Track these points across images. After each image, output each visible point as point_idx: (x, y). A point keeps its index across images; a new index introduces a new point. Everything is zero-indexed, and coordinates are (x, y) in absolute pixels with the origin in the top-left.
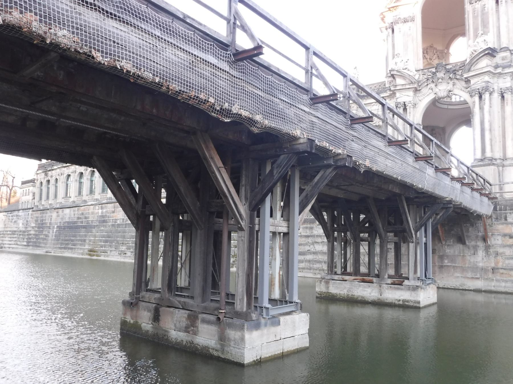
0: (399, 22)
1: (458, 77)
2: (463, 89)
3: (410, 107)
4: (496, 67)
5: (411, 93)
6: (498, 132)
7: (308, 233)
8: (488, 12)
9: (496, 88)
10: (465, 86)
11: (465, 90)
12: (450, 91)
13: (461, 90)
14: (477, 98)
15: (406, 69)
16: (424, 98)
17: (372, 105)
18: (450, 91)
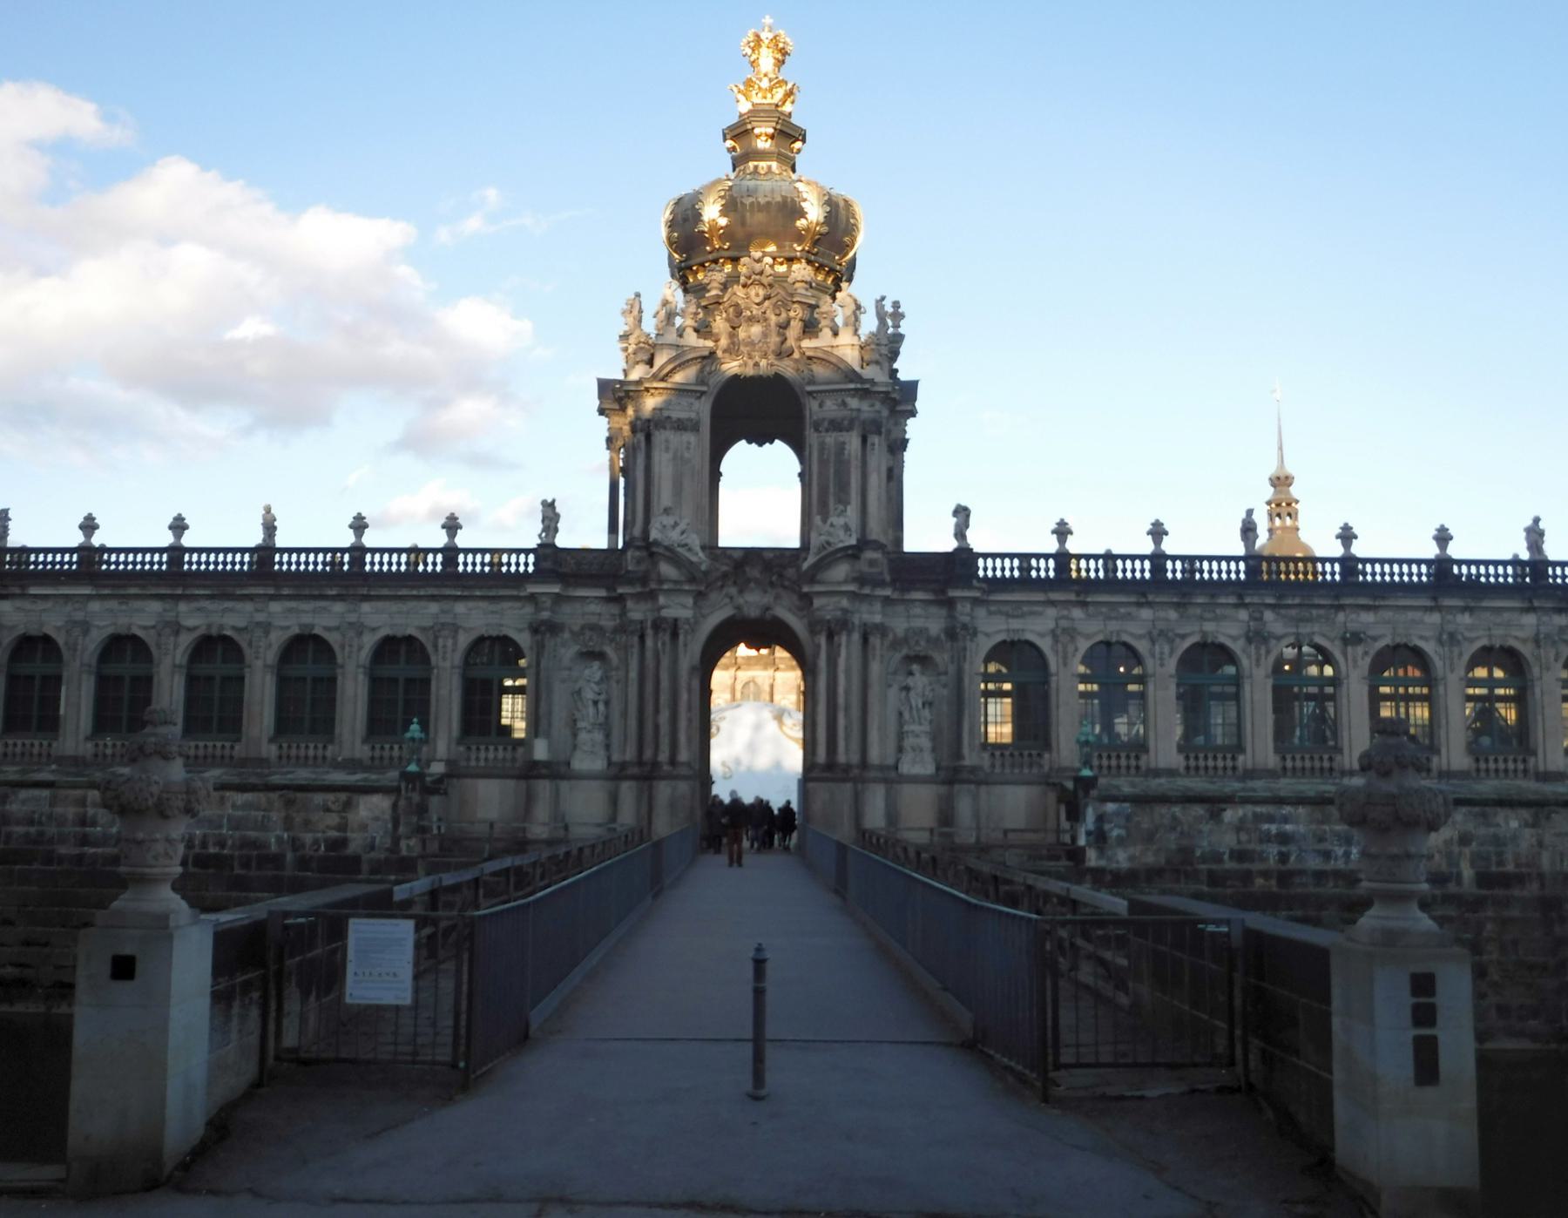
1: (787, 583)
3: (686, 632)
4: (861, 580)
5: (690, 601)
6: (855, 712)
8: (849, 462)
9: (857, 622)
13: (790, 610)
14: (823, 640)
15: (686, 545)
16: (712, 612)
17: (588, 601)
18: (768, 609)
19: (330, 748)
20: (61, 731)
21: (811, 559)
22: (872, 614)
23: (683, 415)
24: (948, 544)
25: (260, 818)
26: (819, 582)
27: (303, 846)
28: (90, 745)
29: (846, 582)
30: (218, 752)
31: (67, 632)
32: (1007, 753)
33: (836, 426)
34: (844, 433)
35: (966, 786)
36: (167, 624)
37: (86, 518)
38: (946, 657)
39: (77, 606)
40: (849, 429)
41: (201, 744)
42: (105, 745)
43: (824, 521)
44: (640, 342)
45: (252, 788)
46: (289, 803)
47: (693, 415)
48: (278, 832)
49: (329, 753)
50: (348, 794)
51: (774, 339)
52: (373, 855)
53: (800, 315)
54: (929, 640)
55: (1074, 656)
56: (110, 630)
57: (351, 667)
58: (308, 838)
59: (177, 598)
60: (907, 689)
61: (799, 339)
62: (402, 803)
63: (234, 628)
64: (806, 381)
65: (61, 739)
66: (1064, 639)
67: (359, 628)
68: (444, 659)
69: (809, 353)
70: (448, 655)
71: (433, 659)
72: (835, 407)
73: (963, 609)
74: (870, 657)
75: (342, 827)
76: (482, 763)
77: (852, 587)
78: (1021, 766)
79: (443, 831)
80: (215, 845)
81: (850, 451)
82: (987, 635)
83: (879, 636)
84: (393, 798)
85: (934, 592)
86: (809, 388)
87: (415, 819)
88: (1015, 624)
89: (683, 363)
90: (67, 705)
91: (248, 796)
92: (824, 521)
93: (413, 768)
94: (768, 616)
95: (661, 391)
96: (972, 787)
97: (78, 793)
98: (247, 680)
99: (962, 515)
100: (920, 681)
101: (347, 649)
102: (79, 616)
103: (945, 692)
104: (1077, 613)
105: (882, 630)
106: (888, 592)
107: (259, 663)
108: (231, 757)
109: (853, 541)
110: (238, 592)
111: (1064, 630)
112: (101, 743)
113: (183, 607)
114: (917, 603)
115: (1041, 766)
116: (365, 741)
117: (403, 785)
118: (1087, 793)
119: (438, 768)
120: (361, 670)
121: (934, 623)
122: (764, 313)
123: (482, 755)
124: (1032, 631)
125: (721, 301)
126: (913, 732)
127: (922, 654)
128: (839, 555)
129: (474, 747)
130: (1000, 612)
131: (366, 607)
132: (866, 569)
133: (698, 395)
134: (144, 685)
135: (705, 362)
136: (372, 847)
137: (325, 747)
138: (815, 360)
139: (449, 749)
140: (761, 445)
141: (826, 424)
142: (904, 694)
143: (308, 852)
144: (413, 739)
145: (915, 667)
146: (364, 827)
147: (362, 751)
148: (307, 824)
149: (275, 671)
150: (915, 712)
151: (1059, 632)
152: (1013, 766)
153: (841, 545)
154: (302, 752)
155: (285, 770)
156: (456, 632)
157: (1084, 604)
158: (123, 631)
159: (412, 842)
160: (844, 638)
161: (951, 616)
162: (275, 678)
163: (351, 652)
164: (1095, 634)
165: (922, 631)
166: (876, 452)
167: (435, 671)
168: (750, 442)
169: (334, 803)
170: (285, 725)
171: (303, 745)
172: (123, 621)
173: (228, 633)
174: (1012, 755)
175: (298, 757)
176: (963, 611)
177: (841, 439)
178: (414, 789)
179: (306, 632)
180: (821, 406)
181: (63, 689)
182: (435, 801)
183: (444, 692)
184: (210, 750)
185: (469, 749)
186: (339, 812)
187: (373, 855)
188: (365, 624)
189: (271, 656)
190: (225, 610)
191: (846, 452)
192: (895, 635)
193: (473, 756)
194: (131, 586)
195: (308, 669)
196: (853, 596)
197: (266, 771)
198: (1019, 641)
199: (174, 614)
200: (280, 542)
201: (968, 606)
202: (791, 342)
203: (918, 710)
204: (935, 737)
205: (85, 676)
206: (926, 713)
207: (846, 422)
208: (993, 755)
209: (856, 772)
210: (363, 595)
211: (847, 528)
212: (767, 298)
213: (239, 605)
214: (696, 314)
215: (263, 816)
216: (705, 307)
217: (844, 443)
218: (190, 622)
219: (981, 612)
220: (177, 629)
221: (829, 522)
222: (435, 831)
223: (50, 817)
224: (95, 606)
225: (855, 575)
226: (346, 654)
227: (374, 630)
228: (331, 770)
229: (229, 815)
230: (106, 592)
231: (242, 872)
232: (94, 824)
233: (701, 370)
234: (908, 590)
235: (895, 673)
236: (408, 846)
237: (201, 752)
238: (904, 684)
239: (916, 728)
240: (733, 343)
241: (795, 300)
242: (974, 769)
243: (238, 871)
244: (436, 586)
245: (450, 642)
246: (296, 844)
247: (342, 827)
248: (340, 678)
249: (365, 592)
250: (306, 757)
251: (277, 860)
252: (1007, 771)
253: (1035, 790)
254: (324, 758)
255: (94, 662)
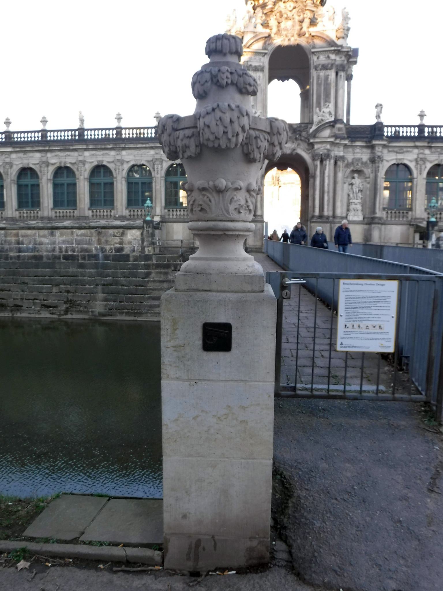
0: (251, 69)
1: (303, 138)
2: (305, 150)
4: (336, 137)
6: (331, 194)
7: (162, 278)
9: (333, 155)
10: (307, 147)
11: (307, 151)
12: (294, 150)
13: (304, 150)
14: (318, 163)
19: (113, 211)
20: (6, 207)
21: (314, 128)
22: (339, 152)
23: (257, 64)
24: (371, 121)
25: (88, 240)
26: (318, 138)
27: (106, 251)
28: (17, 213)
29: (329, 137)
30: (68, 214)
31: (4, 167)
32: (393, 212)
33: (325, 67)
34: (328, 71)
35: (377, 225)
36: (43, 162)
37: (7, 119)
38: (369, 170)
39: (7, 156)
40: (330, 69)
41: (61, 211)
42: (23, 213)
43: (320, 111)
44: (237, 31)
45: (85, 228)
46: (99, 233)
47: (261, 64)
48: (96, 245)
49: (112, 214)
50: (123, 230)
51: (298, 28)
52: (134, 254)
53: (309, 17)
54: (362, 163)
55: (424, 170)
56: (21, 166)
57: (119, 178)
58: (108, 247)
59: (46, 151)
60: (352, 184)
61: (308, 28)
62: (145, 233)
63: (71, 163)
64: (312, 47)
65: (6, 210)
66: (421, 163)
67: (122, 162)
68: (157, 173)
69: (313, 34)
70: (159, 172)
71: (153, 174)
72: (324, 59)
73: (378, 149)
74: (338, 171)
75: (121, 243)
76: (175, 217)
77: (332, 140)
78: (399, 217)
79: (160, 244)
80: (71, 251)
81: (331, 79)
82: (387, 161)
83: (342, 161)
84: (141, 231)
85: (366, 142)
86: (313, 50)
87: (150, 239)
88: (400, 156)
89: (259, 39)
90: (7, 196)
91: (83, 231)
92: (320, 111)
93: (148, 218)
94: (294, 153)
95: (247, 53)
96: (380, 226)
97: (15, 231)
98: (77, 185)
99: (379, 108)
100: (357, 181)
101: (117, 170)
102: (8, 160)
103: (368, 186)
104: (427, 151)
105: (343, 158)
106: (346, 142)
107: (82, 177)
108: (73, 216)
109: (332, 119)
110: (71, 148)
111: (421, 159)
112: (22, 212)
113: (49, 155)
114: (358, 147)
115: (407, 217)
116: (126, 209)
117: (145, 225)
118: (433, 227)
119: (157, 219)
120: (124, 179)
121: (365, 156)
122: (293, 15)
123: (175, 213)
124: (407, 160)
125: (273, 10)
126: (354, 203)
127: (359, 169)
128: (327, 125)
129: (171, 210)
130: (394, 151)
131: (124, 153)
132: (337, 132)
133: (264, 54)
134: (36, 187)
135: (266, 39)
136: (134, 251)
137: (111, 211)
138: (316, 37)
139: (161, 211)
140: (283, 81)
141: (320, 67)
142: (350, 186)
143: (108, 253)
144: (148, 206)
145: (356, 175)
146: (130, 243)
147: (126, 213)
148: (107, 242)
149: (89, 180)
150: (355, 195)
151: (419, 159)
152: (395, 217)
153: (328, 121)
154: (102, 214)
155: (95, 221)
156: (162, 162)
157: (430, 147)
158: (26, 166)
159: (150, 248)
160: (328, 162)
161: (373, 153)
162: (88, 184)
163: (119, 172)
164: (434, 161)
165: (359, 160)
166: (342, 79)
167: (154, 179)
168: (279, 80)
169: (117, 233)
170: (93, 203)
171: (102, 211)
172: (26, 162)
173: (68, 165)
174: (395, 212)
175: (100, 216)
176: (378, 150)
177: (327, 74)
178: (149, 227)
179: (100, 164)
180: (318, 58)
181: (5, 190)
182: (157, 232)
183: (158, 187)
184: (65, 213)
185: (169, 210)
186: (119, 237)
187: (134, 254)
188: (125, 160)
189: (87, 174)
190: (66, 156)
191: (329, 79)
192: (348, 161)
193: (171, 214)
194: (27, 147)
195: (102, 179)
196: (332, 143)
197: (88, 221)
198: (401, 164)
199: (45, 158)
200: (86, 126)
201: (381, 148)
202: (305, 29)
203: (356, 193)
204: (363, 205)
205: (12, 185)
206: (360, 195)
207: (329, 66)
208: (387, 212)
209: (331, 219)
210: (123, 148)
211: (330, 113)
212: (294, 8)
213: (72, 154)
214: (262, 17)
215: (89, 239)
216: (266, 14)
217: (328, 75)
218: (53, 161)
219: (385, 151)
220: (48, 164)
221: (322, 111)
222: (158, 244)
223: (5, 241)
224: (14, 156)
225: (332, 134)
226: (117, 173)
227: (128, 162)
228: (114, 220)
229: (75, 239)
230: (18, 150)
231: (83, 261)
232: (23, 244)
233: (265, 43)
234: (355, 141)
235: (347, 178)
236: (148, 250)
237: (61, 215)
238: (351, 182)
239: (356, 201)
240: (279, 30)
241: (307, 8)
242: (380, 218)
243: (80, 261)
244: (153, 143)
245: (160, 167)
246: (103, 250)
247: (121, 243)
248: (115, 183)
249: (124, 146)
250: (103, 216)
251: (96, 257)
252: (393, 219)
253: (404, 228)
254: (111, 216)
255: (16, 179)
